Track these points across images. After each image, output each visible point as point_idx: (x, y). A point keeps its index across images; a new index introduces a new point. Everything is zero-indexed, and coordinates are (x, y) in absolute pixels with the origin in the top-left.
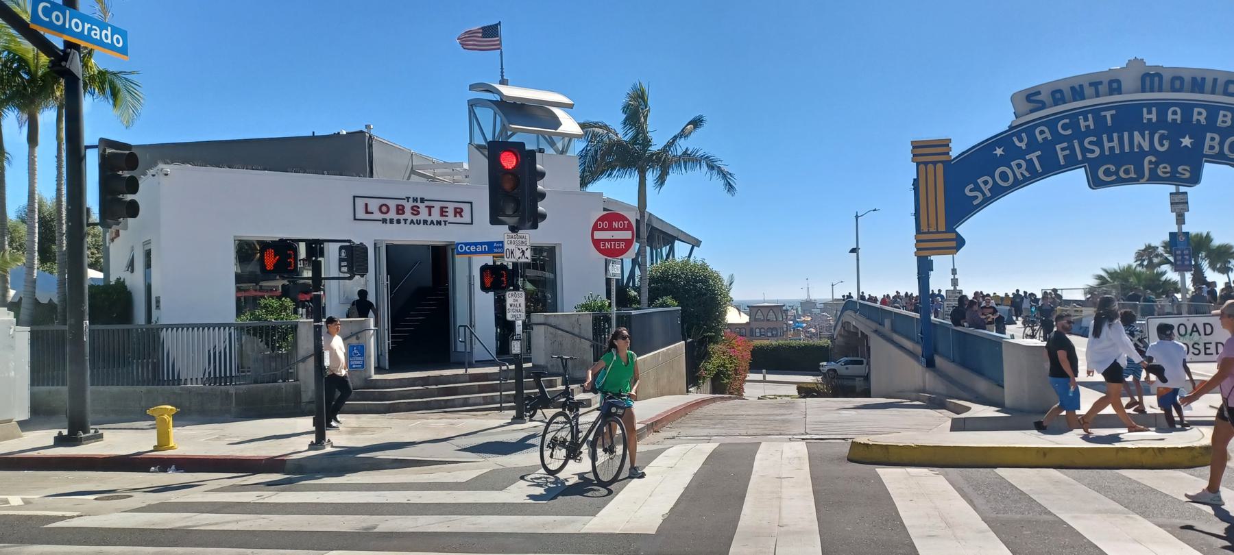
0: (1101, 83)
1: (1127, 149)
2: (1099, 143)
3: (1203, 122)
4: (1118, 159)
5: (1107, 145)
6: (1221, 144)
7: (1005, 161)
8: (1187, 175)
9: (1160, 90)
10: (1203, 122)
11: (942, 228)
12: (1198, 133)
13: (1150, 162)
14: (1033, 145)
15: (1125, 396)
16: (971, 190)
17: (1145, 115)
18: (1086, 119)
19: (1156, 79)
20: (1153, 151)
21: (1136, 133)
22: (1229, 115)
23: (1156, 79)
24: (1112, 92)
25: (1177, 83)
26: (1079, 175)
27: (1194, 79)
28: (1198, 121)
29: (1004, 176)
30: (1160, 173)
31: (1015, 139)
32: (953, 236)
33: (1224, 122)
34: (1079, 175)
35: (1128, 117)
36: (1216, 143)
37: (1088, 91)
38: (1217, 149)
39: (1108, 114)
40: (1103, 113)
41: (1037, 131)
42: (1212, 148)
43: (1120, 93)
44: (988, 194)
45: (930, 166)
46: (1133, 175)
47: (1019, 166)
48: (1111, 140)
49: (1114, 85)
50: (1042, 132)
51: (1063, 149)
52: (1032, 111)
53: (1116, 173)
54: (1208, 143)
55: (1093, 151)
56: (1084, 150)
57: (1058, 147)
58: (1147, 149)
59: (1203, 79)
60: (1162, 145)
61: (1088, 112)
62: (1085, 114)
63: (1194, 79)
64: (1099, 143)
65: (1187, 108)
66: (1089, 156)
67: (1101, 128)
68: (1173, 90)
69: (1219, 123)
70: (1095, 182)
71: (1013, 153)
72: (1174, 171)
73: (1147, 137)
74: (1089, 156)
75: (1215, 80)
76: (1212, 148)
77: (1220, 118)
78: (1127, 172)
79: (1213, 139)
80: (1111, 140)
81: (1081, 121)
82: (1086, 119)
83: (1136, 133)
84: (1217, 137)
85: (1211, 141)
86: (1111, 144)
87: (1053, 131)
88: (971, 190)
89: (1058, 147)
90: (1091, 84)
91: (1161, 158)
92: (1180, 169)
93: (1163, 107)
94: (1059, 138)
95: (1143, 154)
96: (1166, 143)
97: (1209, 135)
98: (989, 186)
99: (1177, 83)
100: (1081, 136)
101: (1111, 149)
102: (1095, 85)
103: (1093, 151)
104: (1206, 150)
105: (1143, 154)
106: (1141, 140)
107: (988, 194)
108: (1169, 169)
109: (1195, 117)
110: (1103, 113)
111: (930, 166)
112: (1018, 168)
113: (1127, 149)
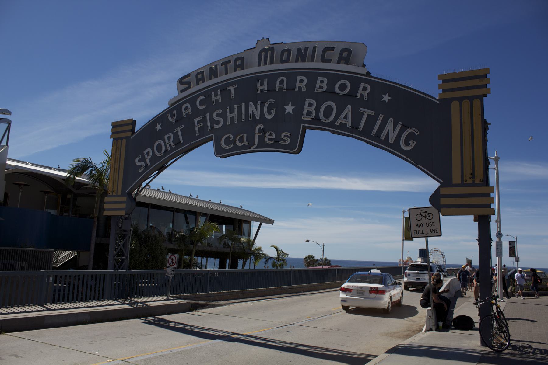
0: (229, 62)
1: (243, 117)
2: (223, 115)
3: (304, 89)
5: (229, 115)
6: (317, 110)
7: (160, 135)
8: (288, 141)
9: (272, 63)
10: (304, 89)
11: (120, 193)
12: (298, 99)
15: (443, 324)
16: (139, 161)
17: (260, 87)
18: (216, 95)
19: (269, 52)
20: (263, 119)
21: (251, 103)
22: (326, 80)
23: (269, 52)
24: (236, 68)
25: (286, 54)
26: (210, 146)
27: (299, 50)
29: (159, 147)
30: (266, 139)
31: (169, 116)
33: (321, 87)
34: (210, 146)
35: (247, 89)
36: (313, 109)
37: (220, 68)
38: (314, 114)
40: (229, 88)
41: (183, 108)
42: (309, 113)
44: (149, 163)
45: (120, 141)
46: (245, 143)
47: (169, 138)
48: (232, 112)
49: (239, 62)
50: (186, 108)
51: (199, 122)
52: (182, 91)
55: (218, 122)
56: (213, 122)
57: (196, 120)
58: (258, 118)
59: (306, 49)
60: (270, 113)
62: (215, 90)
63: (299, 50)
64: (223, 115)
65: (291, 76)
66: (216, 126)
68: (282, 61)
69: (317, 90)
70: (220, 152)
71: (168, 128)
74: (216, 126)
75: (315, 48)
76: (309, 113)
77: (318, 85)
79: (310, 105)
80: (232, 112)
81: (213, 96)
82: (216, 95)
83: (251, 103)
85: (310, 106)
86: (232, 115)
87: (194, 106)
88: (139, 161)
89: (196, 120)
90: (222, 64)
92: (283, 135)
93: (272, 77)
94: (196, 112)
95: (255, 122)
96: (273, 111)
97: (307, 102)
98: (149, 157)
99: (286, 54)
101: (232, 119)
102: (225, 63)
103: (218, 122)
105: (255, 122)
106: (254, 110)
107: (149, 163)
108: (274, 137)
109: (298, 85)
110: (229, 88)
111: (120, 141)
112: (168, 141)
113: (243, 117)
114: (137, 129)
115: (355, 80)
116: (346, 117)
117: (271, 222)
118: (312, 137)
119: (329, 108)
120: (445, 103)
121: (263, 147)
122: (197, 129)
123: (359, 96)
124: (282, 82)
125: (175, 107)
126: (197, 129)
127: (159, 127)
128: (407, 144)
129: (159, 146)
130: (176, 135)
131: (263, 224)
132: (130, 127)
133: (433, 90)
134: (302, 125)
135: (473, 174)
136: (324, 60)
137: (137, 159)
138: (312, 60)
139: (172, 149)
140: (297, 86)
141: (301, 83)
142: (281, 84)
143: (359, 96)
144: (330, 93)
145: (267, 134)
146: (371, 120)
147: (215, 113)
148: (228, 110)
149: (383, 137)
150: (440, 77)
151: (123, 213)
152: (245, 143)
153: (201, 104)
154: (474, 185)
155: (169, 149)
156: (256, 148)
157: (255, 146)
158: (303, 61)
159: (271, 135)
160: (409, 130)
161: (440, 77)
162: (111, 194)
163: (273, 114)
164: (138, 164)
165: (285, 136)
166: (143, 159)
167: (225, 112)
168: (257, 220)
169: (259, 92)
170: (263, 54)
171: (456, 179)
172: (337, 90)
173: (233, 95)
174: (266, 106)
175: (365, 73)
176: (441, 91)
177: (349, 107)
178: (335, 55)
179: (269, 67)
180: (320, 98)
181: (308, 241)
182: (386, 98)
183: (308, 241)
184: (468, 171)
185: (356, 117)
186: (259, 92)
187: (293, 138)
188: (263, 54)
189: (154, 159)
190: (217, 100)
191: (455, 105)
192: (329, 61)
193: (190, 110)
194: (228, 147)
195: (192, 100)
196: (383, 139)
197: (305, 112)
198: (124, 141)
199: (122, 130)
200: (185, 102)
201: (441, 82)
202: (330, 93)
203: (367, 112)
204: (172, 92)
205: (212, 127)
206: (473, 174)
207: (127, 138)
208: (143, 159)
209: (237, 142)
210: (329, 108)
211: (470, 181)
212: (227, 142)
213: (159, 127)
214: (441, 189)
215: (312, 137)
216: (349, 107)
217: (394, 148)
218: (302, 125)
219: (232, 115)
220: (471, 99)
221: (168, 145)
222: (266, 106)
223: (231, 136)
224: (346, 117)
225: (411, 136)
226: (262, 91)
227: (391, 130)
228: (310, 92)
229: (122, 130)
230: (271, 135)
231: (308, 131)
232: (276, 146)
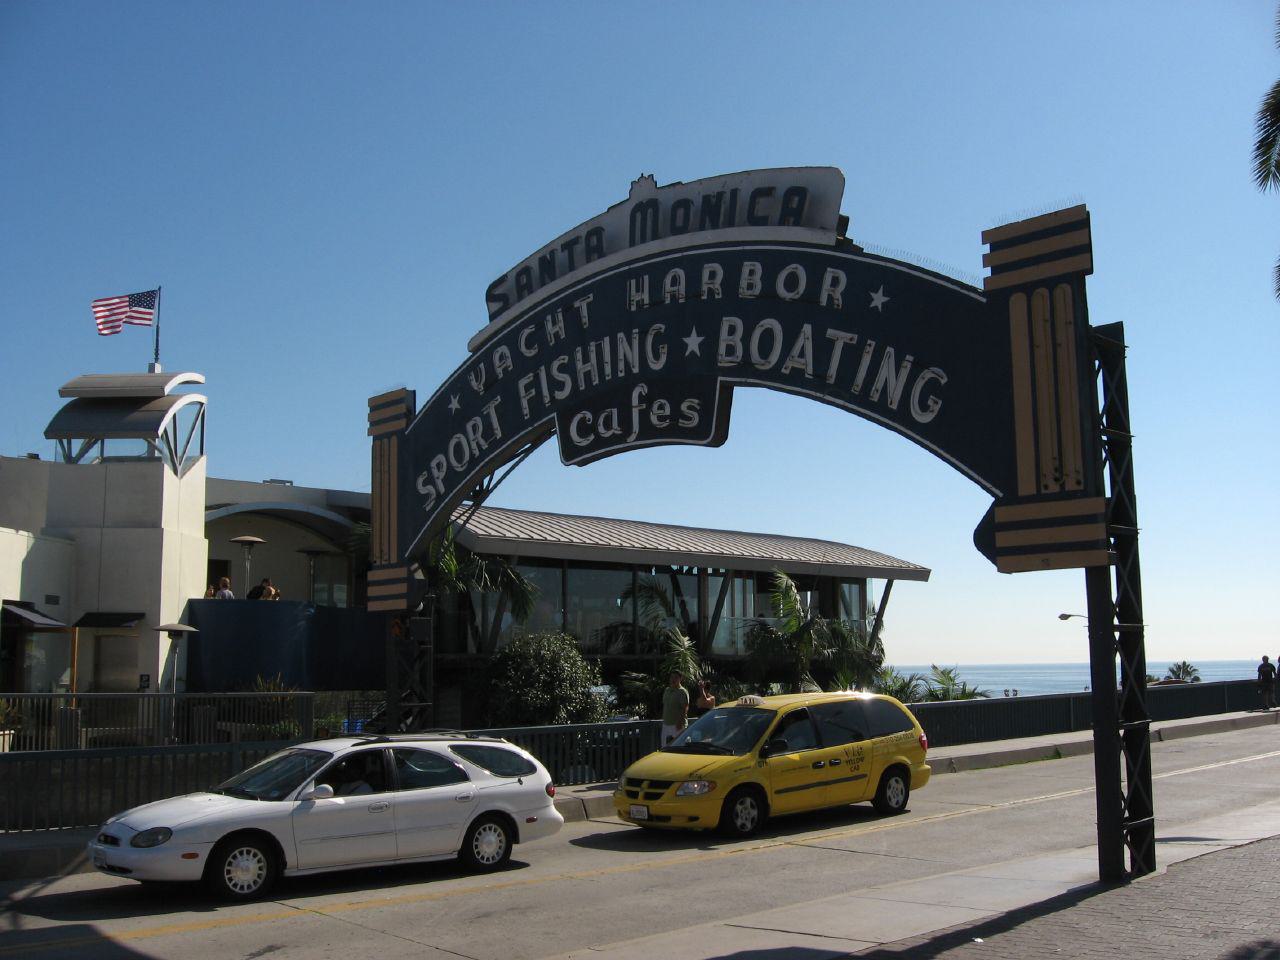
1: (608, 369)
4: (608, 395)
7: (458, 423)
11: (394, 560)
13: (641, 398)
14: (492, 383)
16: (425, 484)
17: (636, 297)
19: (650, 211)
20: (646, 374)
21: (621, 335)
23: (650, 211)
25: (681, 212)
28: (711, 292)
30: (654, 420)
32: (402, 573)
33: (750, 286)
37: (561, 257)
38: (740, 351)
39: (582, 305)
40: (577, 304)
41: (496, 357)
43: (601, 255)
47: (475, 428)
48: (586, 360)
49: (591, 240)
50: (502, 357)
51: (527, 388)
53: (593, 429)
54: (724, 338)
55: (561, 386)
57: (522, 383)
61: (555, 306)
67: (578, 336)
68: (677, 231)
69: (744, 292)
71: (473, 405)
72: (677, 414)
73: (636, 343)
76: (730, 350)
78: (608, 425)
79: (732, 330)
81: (549, 326)
83: (621, 335)
84: (739, 323)
86: (588, 367)
88: (425, 484)
91: (661, 386)
92: (684, 407)
93: (656, 271)
95: (631, 381)
96: (664, 350)
97: (727, 322)
99: (681, 212)
100: (545, 357)
104: (724, 361)
105: (631, 381)
106: (629, 351)
107: (442, 489)
108: (668, 411)
113: (608, 369)
114: (418, 409)
115: (816, 265)
116: (802, 355)
117: (922, 574)
118: (750, 404)
119: (768, 335)
120: (996, 296)
121: (652, 436)
122: (525, 403)
123: (824, 301)
124: (675, 281)
125: (483, 350)
126: (525, 403)
127: (455, 404)
128: (924, 407)
129: (458, 447)
130: (487, 420)
131: (896, 583)
132: (402, 409)
133: (970, 268)
134: (720, 379)
135: (1060, 469)
136: (755, 220)
137: (420, 480)
138: (730, 223)
139: (484, 453)
140: (705, 288)
141: (712, 278)
142: (675, 285)
143: (824, 301)
144: (768, 303)
145: (655, 406)
146: (852, 355)
147: (556, 364)
148: (579, 356)
149: (875, 397)
150: (987, 236)
151: (402, 604)
152: (616, 429)
153: (529, 346)
154: (1064, 495)
155: (477, 453)
156: (637, 440)
157: (633, 436)
158: (715, 226)
159: (661, 407)
160: (927, 375)
161: (987, 236)
162: (378, 563)
163: (663, 359)
164: (423, 490)
165: (689, 408)
166: (430, 481)
167: (572, 360)
168: (878, 572)
169: (633, 308)
170: (639, 216)
171: (1026, 487)
172: (781, 291)
173: (585, 320)
174: (650, 340)
175: (832, 243)
176: (987, 272)
177: (807, 329)
178: (770, 207)
179: (653, 247)
180: (751, 313)
181: (1064, 617)
182: (879, 299)
183: (1064, 617)
184: (1048, 466)
185: (823, 348)
186: (633, 308)
187: (705, 413)
188: (639, 216)
189: (452, 478)
190: (556, 335)
191: (1017, 305)
192: (762, 221)
193: (509, 362)
194: (584, 443)
195: (511, 340)
196: (876, 400)
197: (722, 350)
198: (394, 439)
199: (392, 417)
200: (498, 344)
201: (986, 249)
202: (768, 303)
203: (841, 338)
204: (477, 319)
205: (552, 398)
206: (1060, 469)
207: (400, 433)
208: (430, 481)
209: (601, 429)
210: (768, 335)
211: (1054, 488)
212: (583, 430)
213: (455, 404)
214: (996, 509)
215: (750, 404)
216: (807, 329)
217: (897, 418)
218: (720, 379)
219: (588, 367)
220: (1051, 283)
221: (474, 445)
222: (650, 340)
223: (589, 415)
224: (802, 355)
225: (932, 387)
226: (640, 304)
227: (892, 378)
228: (731, 302)
229: (392, 417)
230: (661, 407)
231: (738, 391)
232: (675, 433)
